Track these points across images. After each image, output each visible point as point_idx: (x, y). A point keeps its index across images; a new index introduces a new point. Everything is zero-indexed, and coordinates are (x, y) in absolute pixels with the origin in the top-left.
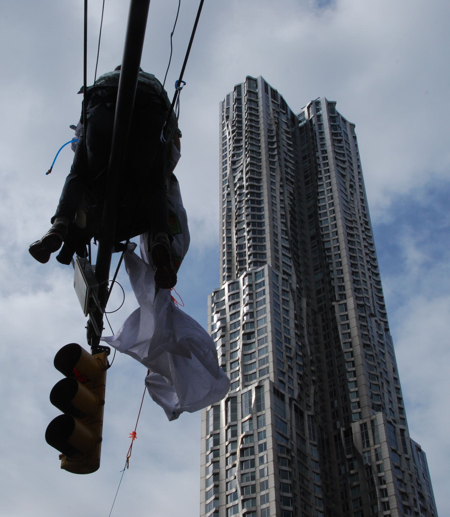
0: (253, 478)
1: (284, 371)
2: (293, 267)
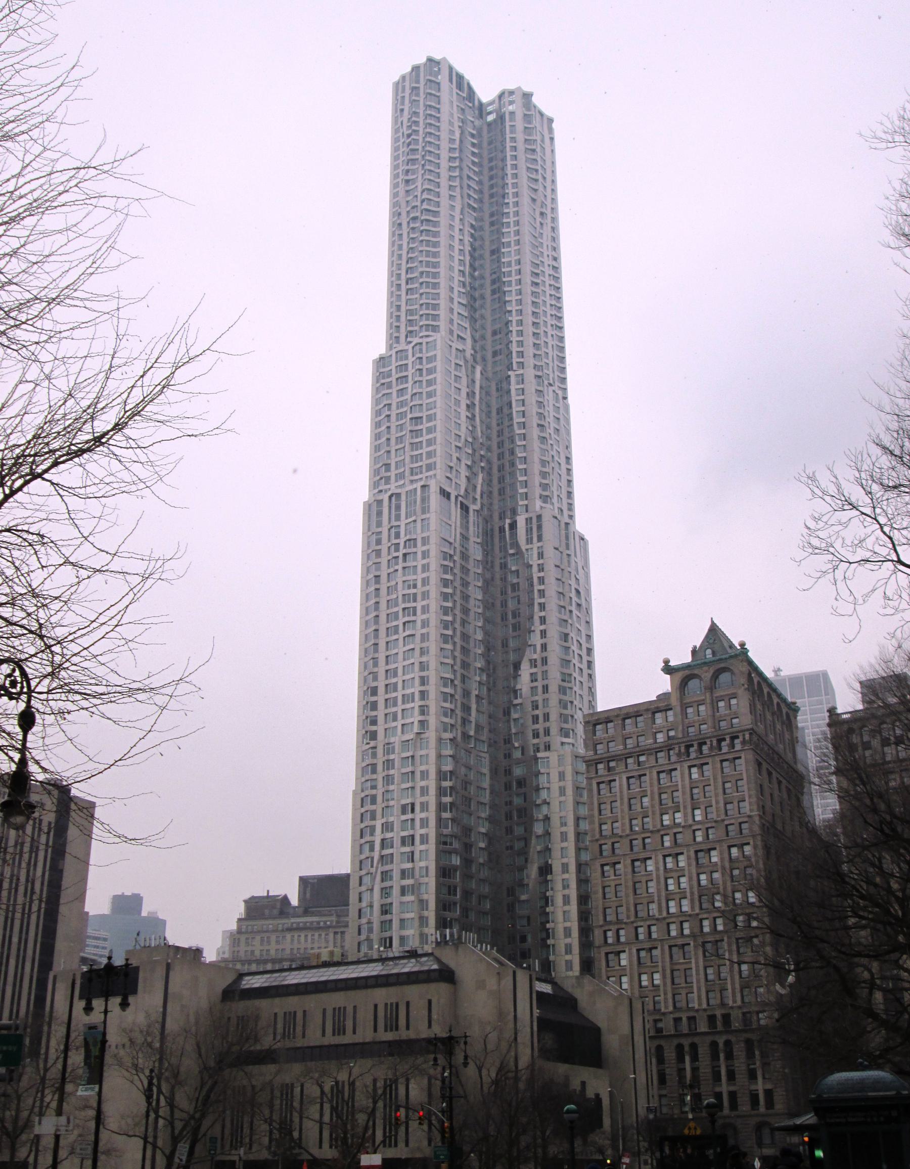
0: (415, 586)
1: (452, 465)
2: (468, 330)
